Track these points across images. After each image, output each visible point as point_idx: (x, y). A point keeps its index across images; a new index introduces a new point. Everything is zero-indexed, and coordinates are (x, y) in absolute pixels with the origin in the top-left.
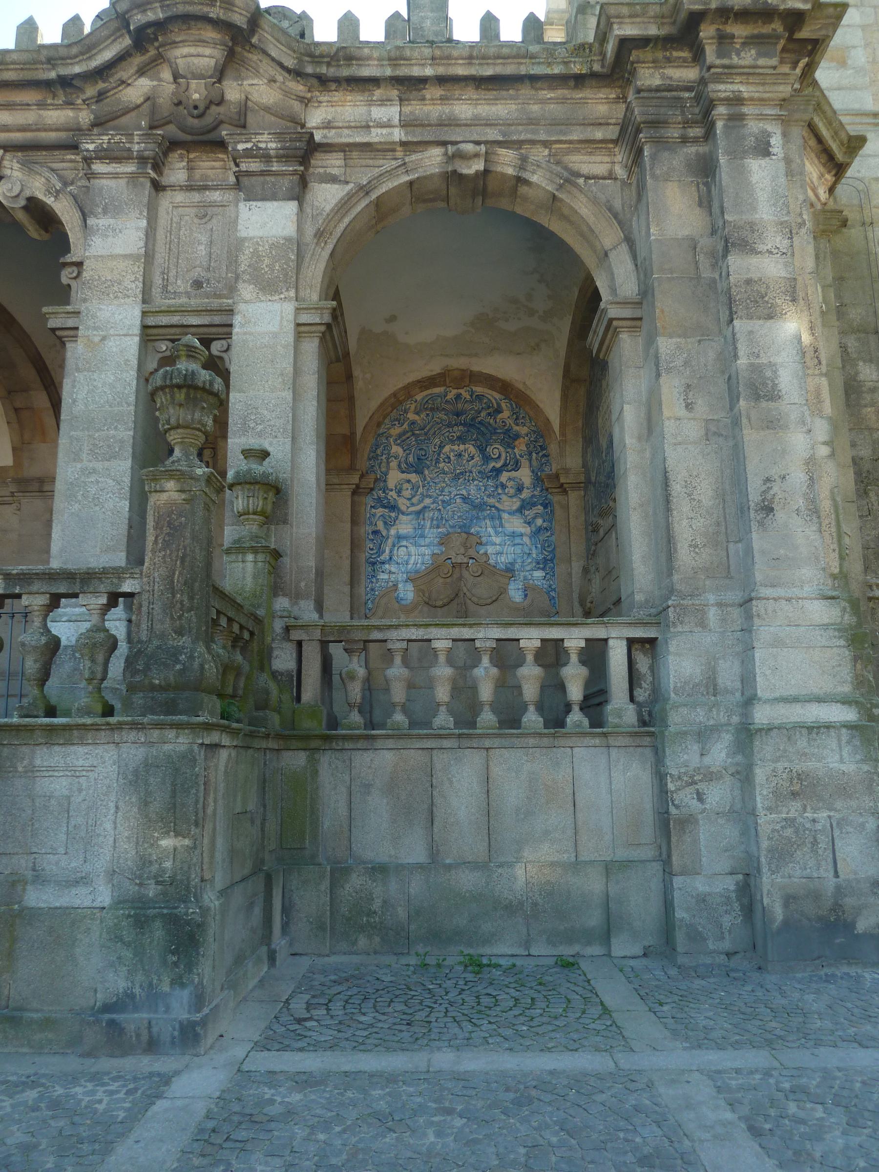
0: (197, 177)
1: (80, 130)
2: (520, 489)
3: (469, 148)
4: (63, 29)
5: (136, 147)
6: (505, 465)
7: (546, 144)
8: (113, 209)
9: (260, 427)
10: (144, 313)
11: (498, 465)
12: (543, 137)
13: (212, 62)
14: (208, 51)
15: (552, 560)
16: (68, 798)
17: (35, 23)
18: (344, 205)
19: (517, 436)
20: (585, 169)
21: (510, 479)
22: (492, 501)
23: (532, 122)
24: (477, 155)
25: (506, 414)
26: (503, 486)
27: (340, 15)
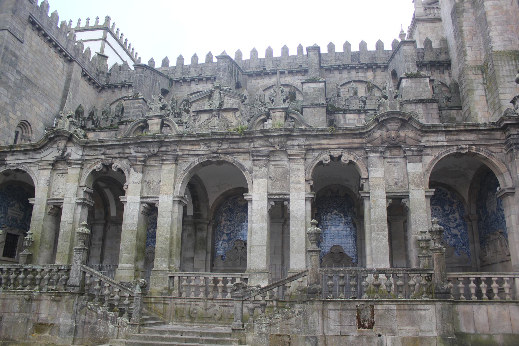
0: (393, 154)
1: (363, 144)
2: (456, 220)
3: (464, 146)
4: (266, 53)
5: (380, 149)
6: (450, 212)
7: (484, 145)
8: (375, 165)
9: (419, 223)
10: (386, 193)
11: (448, 212)
12: (483, 143)
13: (397, 127)
14: (396, 124)
15: (468, 243)
16: (425, 315)
17: (256, 50)
18: (432, 162)
19: (453, 203)
20: (494, 151)
21: (452, 217)
22: (447, 224)
23: (481, 140)
24: (466, 148)
25: (449, 196)
26: (450, 219)
27: (359, 42)
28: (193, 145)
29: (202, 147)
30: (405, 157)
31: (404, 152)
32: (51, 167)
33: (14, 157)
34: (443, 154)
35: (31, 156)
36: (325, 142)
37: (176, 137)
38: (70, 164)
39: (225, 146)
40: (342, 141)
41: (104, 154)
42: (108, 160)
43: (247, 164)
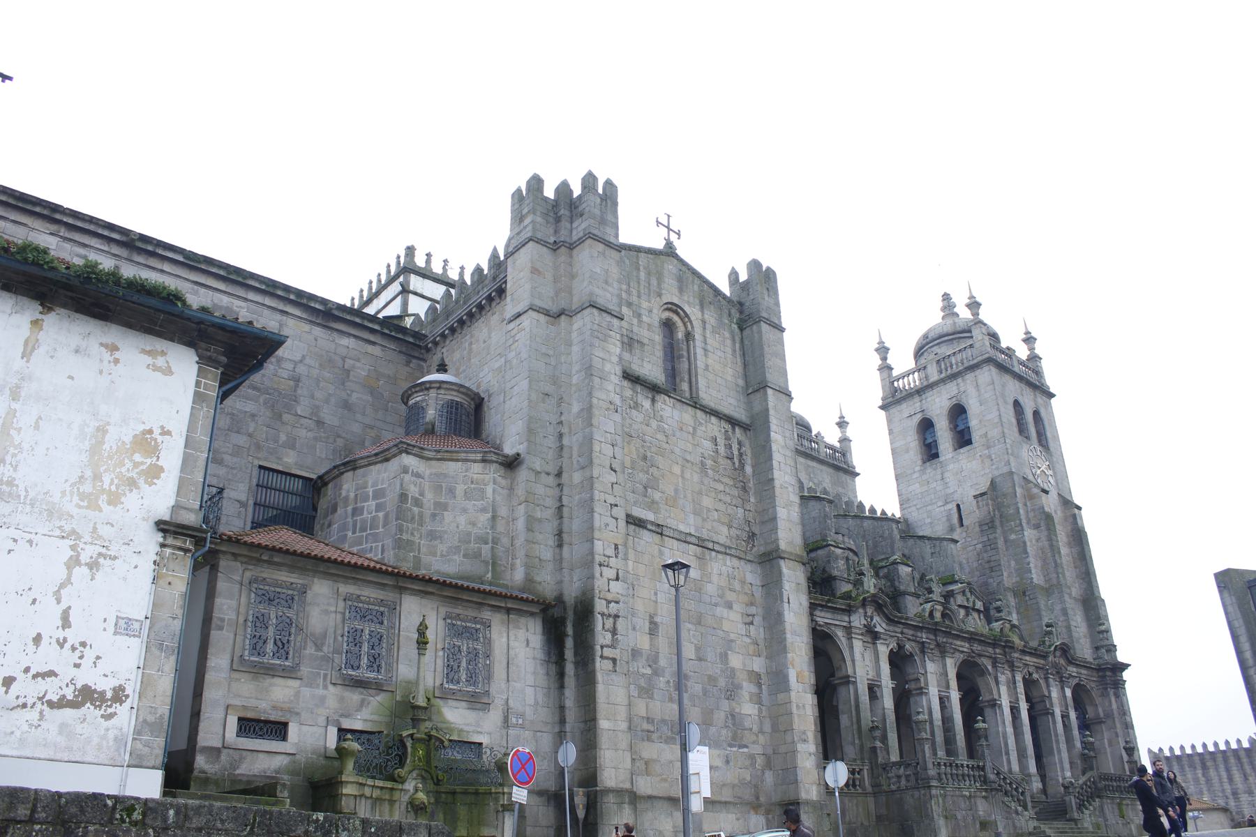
28: (962, 641)
29: (967, 645)
30: (1061, 681)
31: (1061, 678)
32: (860, 637)
33: (823, 614)
34: (1076, 681)
35: (839, 618)
36: (1028, 658)
37: (958, 631)
38: (880, 638)
39: (979, 648)
40: (1035, 660)
41: (902, 633)
42: (902, 640)
43: (990, 668)
